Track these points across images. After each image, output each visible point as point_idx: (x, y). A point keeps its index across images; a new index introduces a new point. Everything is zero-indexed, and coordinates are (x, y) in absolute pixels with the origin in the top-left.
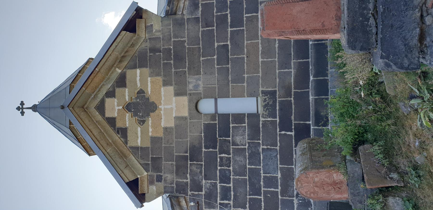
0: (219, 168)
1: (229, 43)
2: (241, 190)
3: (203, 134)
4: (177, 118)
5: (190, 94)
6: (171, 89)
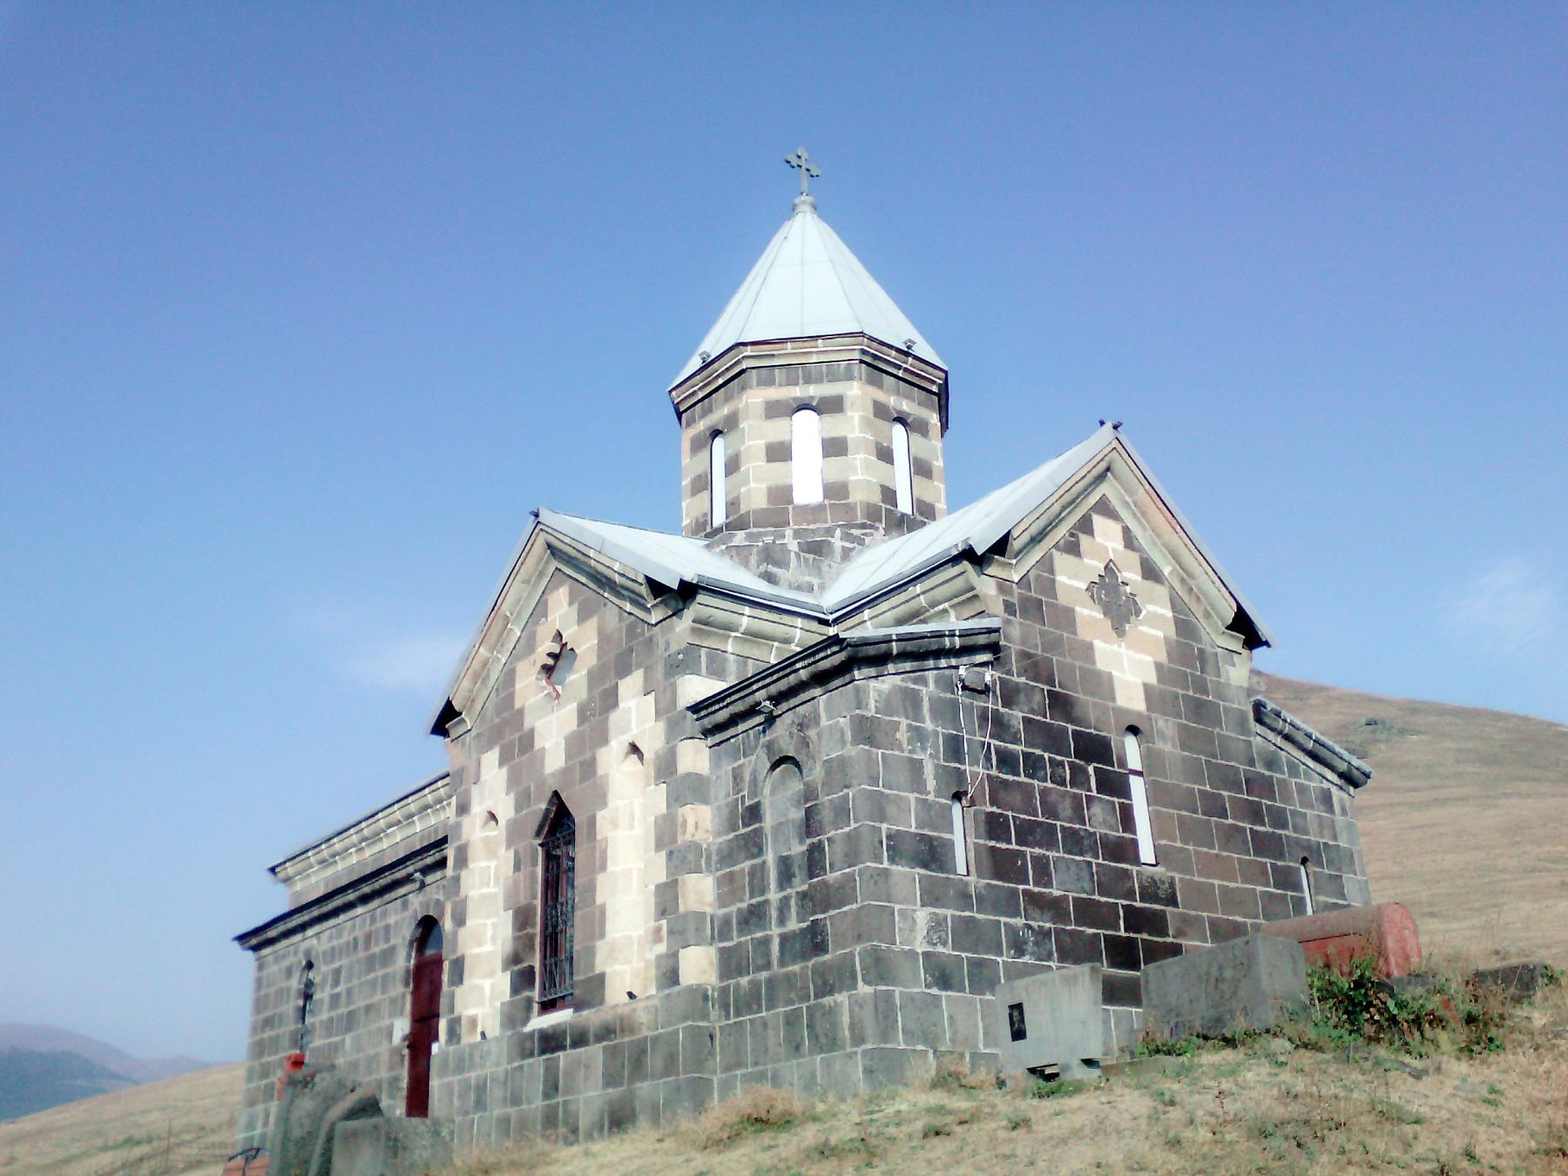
0: (1046, 755)
1: (1230, 821)
2: (1016, 798)
6: (1152, 679)
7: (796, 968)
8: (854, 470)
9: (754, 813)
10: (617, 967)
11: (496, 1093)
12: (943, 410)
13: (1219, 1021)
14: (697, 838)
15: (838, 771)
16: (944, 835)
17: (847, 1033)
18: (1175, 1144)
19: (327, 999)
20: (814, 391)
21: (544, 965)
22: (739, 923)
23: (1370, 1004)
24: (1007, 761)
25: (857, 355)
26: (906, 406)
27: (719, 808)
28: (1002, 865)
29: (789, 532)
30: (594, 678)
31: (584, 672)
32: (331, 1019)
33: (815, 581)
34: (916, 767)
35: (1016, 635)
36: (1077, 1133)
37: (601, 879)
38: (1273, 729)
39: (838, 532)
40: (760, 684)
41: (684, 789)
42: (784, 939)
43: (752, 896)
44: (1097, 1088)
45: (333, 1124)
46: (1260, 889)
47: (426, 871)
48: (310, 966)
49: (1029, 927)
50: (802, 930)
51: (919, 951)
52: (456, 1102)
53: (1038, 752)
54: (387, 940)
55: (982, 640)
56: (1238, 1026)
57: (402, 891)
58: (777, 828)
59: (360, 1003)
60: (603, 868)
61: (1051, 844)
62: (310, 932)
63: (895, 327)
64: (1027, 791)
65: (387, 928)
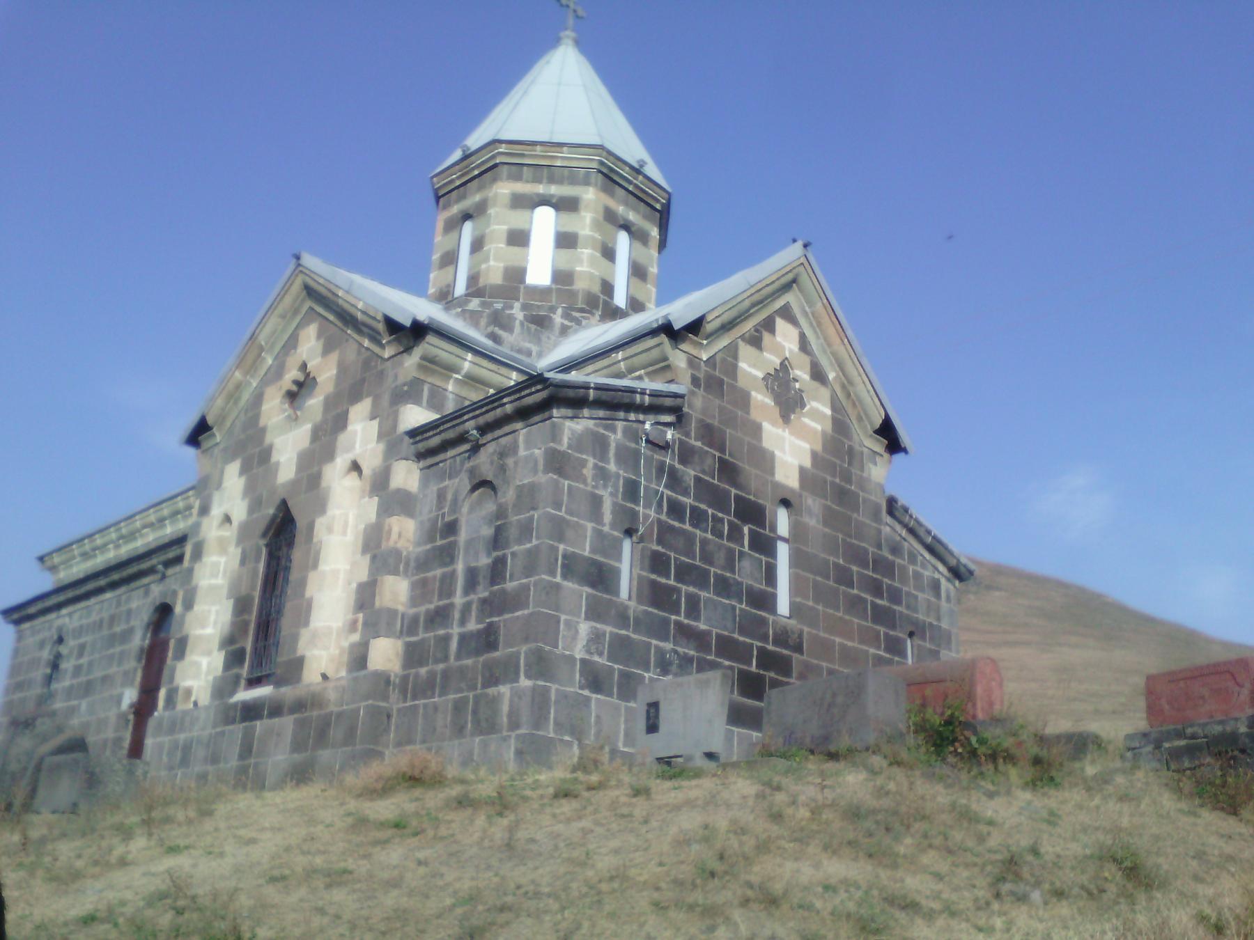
0: (710, 511)
1: (855, 591)
2: (680, 542)
3: (751, 497)
4: (772, 455)
5: (801, 496)
6: (807, 463)
7: (469, 662)
8: (580, 261)
9: (451, 528)
10: (316, 652)
11: (200, 753)
12: (663, 226)
13: (826, 739)
14: (399, 545)
15: (528, 496)
16: (612, 562)
17: (505, 719)
18: (777, 817)
19: (71, 669)
20: (554, 190)
21: (255, 650)
22: (426, 621)
23: (955, 740)
24: (676, 510)
25: (595, 165)
26: (632, 216)
27: (422, 523)
28: (659, 596)
29: (517, 305)
30: (329, 403)
31: (321, 398)
32: (72, 687)
33: (534, 349)
34: (596, 502)
35: (697, 406)
36: (690, 804)
37: (312, 577)
38: (900, 522)
39: (560, 311)
40: (471, 415)
41: (394, 502)
42: (463, 638)
43: (440, 598)
44: (714, 775)
45: (42, 759)
46: (872, 651)
47: (168, 564)
48: (60, 640)
49: (676, 652)
50: (479, 631)
51: (578, 656)
52: (165, 758)
53: (703, 506)
54: (128, 621)
55: (668, 402)
56: (844, 742)
57: (146, 580)
58: (470, 543)
59: (98, 674)
60: (315, 566)
61: (703, 584)
62: (64, 611)
63: (629, 147)
64: (690, 538)
65: (129, 612)
